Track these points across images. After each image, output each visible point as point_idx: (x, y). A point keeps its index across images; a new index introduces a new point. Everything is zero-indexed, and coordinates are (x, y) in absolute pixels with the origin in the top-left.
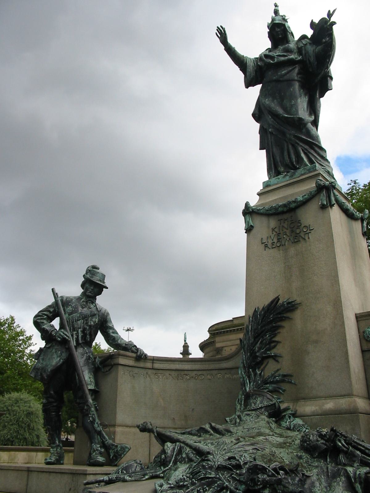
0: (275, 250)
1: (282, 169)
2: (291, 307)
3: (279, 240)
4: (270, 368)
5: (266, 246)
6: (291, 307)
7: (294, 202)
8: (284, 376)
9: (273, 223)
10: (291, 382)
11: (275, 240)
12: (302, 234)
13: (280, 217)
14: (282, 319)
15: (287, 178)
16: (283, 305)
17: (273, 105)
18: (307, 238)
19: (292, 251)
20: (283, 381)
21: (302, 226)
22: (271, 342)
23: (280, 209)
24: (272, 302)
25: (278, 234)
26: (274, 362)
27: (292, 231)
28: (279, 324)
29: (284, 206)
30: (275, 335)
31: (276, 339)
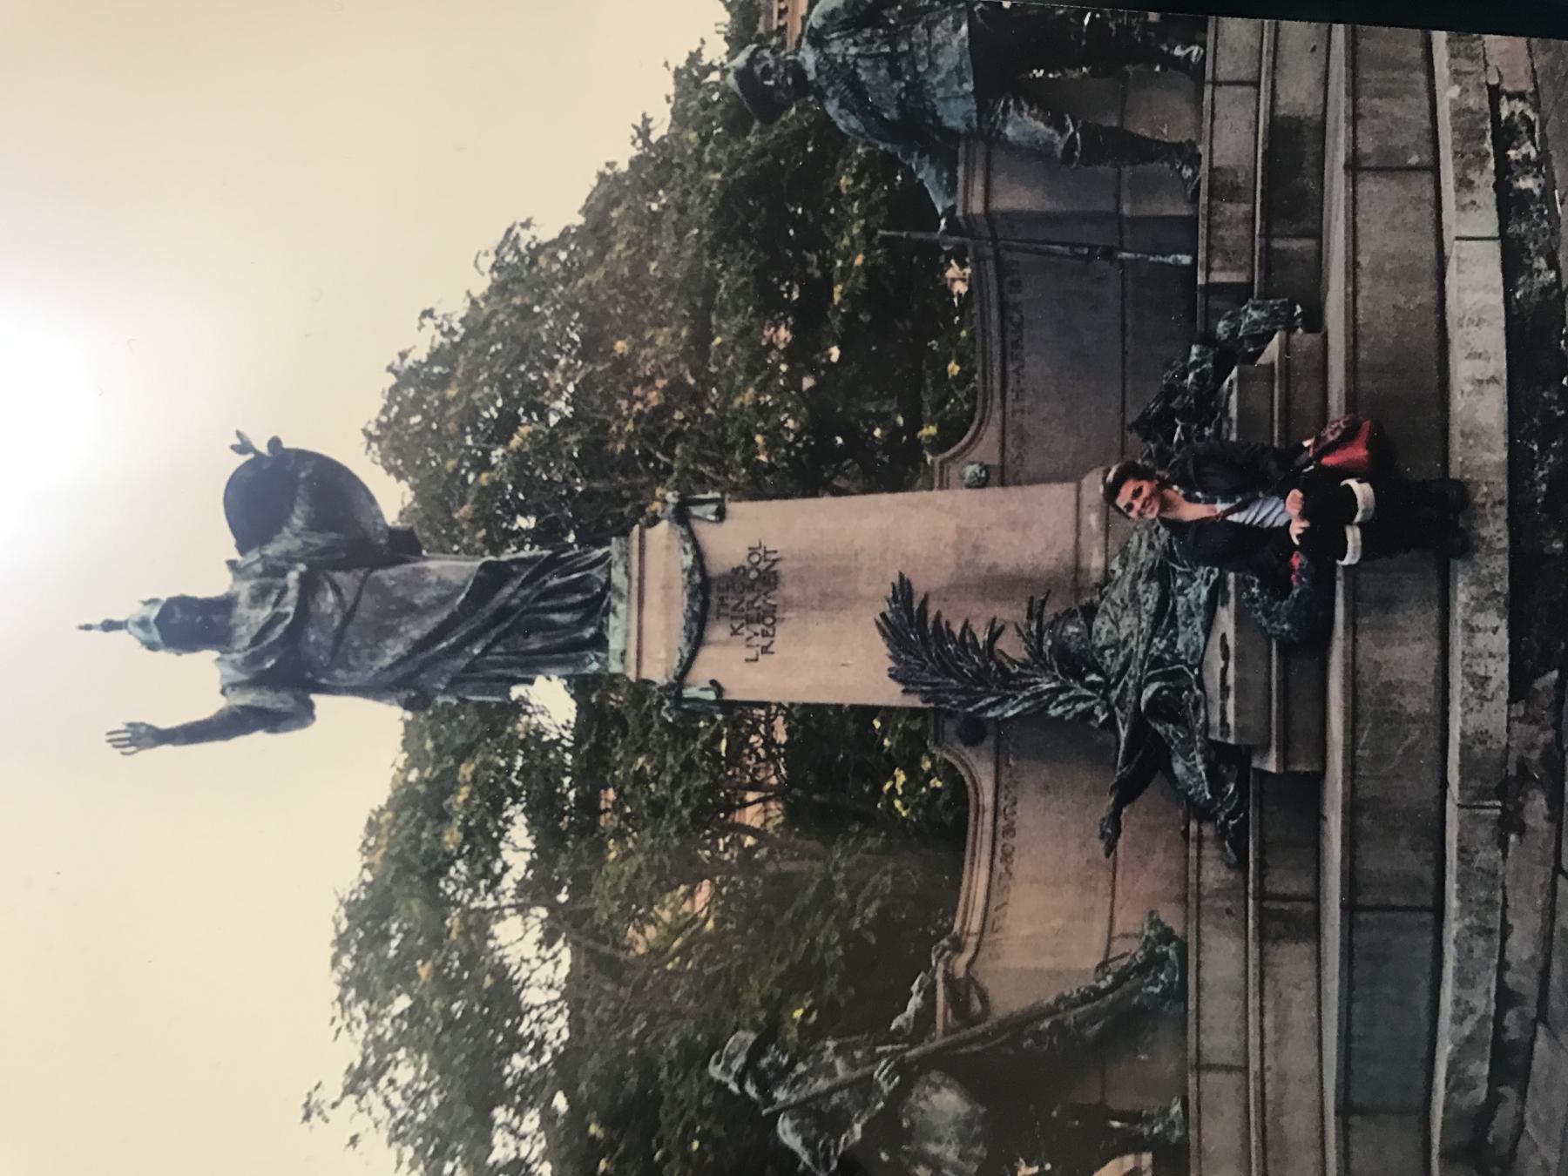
0: (779, 628)
1: (588, 632)
2: (903, 591)
3: (760, 620)
4: (1012, 647)
5: (765, 650)
6: (903, 591)
9: (718, 632)
11: (759, 628)
13: (712, 616)
15: (621, 607)
17: (416, 634)
19: (789, 590)
25: (749, 621)
26: (1003, 637)
29: (692, 596)
30: (951, 633)
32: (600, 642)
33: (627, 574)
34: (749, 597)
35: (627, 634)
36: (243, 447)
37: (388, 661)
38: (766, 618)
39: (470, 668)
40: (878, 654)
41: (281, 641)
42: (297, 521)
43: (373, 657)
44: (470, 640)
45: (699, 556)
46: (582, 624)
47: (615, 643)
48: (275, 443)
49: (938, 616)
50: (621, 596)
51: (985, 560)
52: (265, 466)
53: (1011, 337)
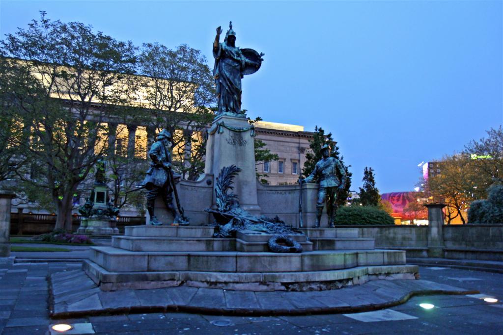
0: (232, 146)
1: (229, 108)
2: (239, 170)
3: (234, 142)
4: (229, 192)
5: (228, 143)
6: (239, 170)
8: (235, 195)
9: (232, 134)
11: (232, 142)
13: (235, 133)
14: (235, 174)
15: (234, 115)
17: (231, 78)
19: (239, 148)
20: (234, 197)
22: (230, 182)
23: (236, 130)
24: (232, 166)
25: (234, 140)
26: (231, 190)
29: (239, 129)
30: (231, 179)
31: (232, 181)
32: (227, 111)
33: (240, 117)
34: (238, 140)
35: (230, 116)
36: (262, 54)
37: (226, 73)
38: (234, 143)
39: (223, 86)
40: (228, 165)
41: (230, 56)
42: (247, 60)
43: (227, 71)
44: (229, 87)
45: (245, 131)
46: (231, 108)
47: (228, 113)
48: (263, 60)
49: (234, 177)
50: (236, 115)
51: (244, 186)
52: (259, 58)
53: (279, 192)
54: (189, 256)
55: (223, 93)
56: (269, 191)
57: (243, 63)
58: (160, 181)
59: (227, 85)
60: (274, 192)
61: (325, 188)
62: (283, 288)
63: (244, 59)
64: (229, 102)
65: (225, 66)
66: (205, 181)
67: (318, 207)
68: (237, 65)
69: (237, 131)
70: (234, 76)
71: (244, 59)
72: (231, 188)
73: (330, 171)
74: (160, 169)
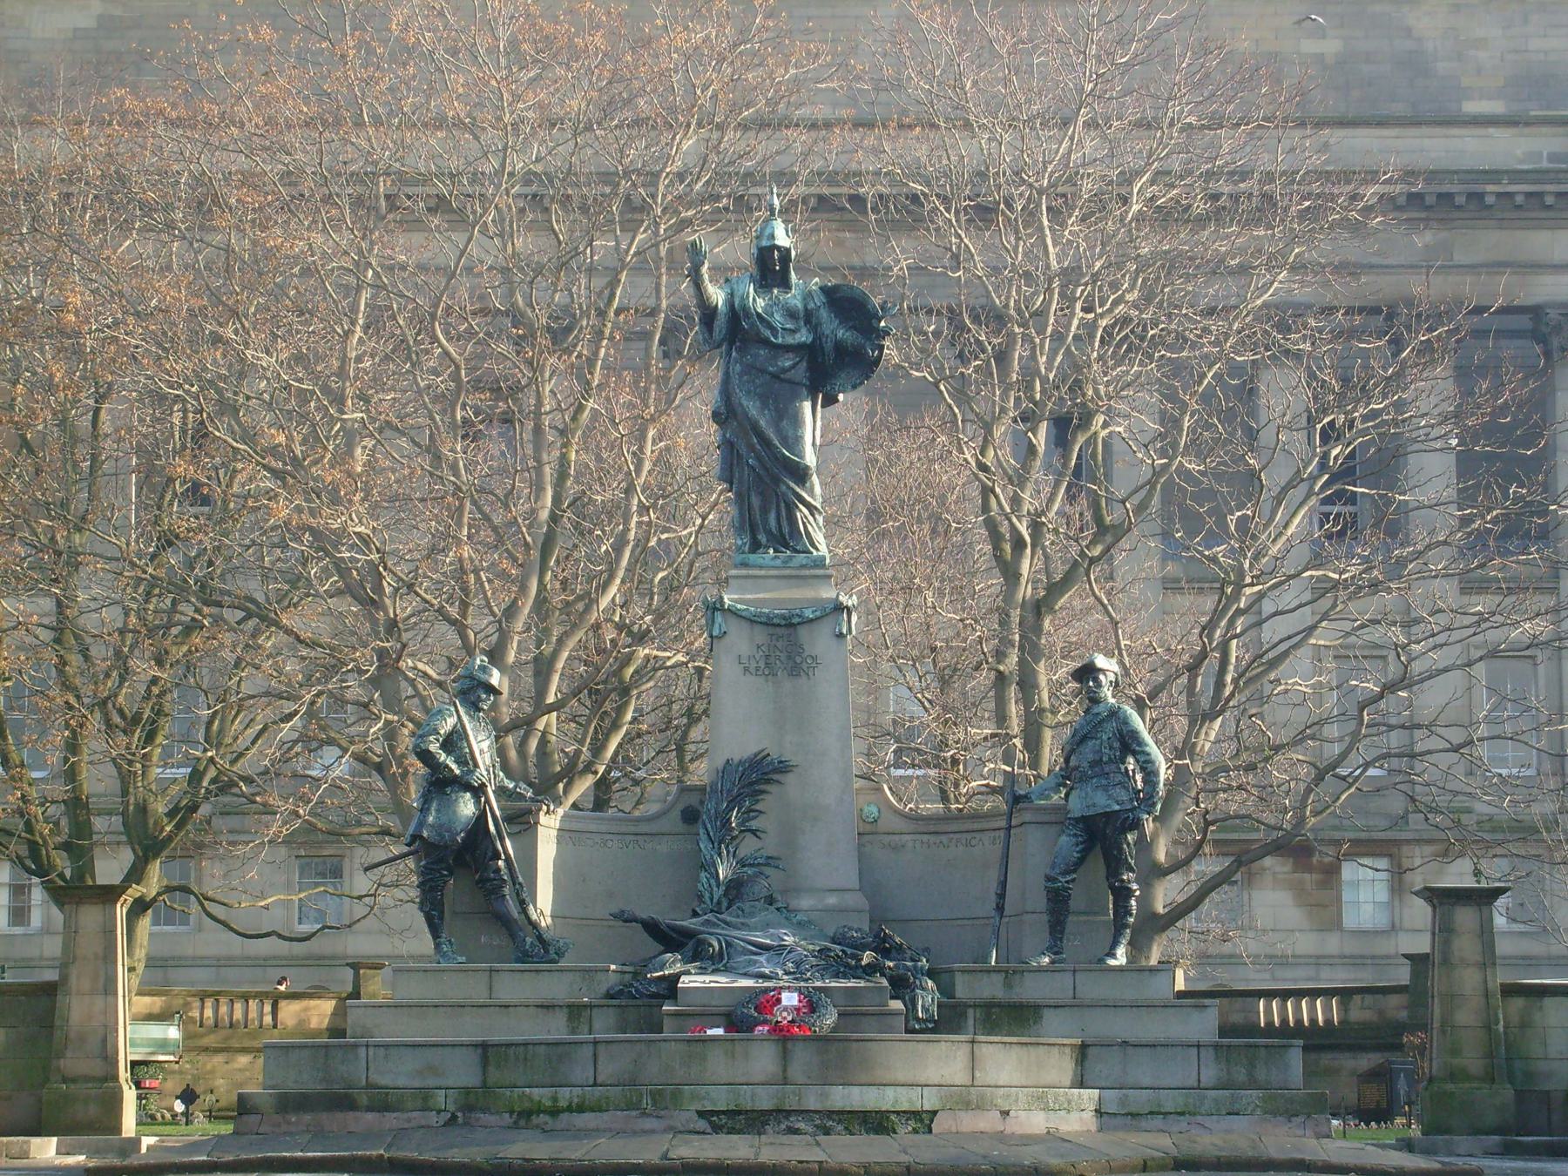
0: (761, 680)
1: (762, 538)
5: (746, 670)
6: (783, 768)
7: (800, 616)
9: (761, 635)
10: (777, 867)
12: (805, 666)
13: (771, 630)
14: (768, 781)
16: (772, 763)
17: (762, 423)
18: (811, 674)
20: (768, 865)
21: (805, 655)
23: (775, 621)
25: (767, 657)
27: (789, 658)
28: (763, 787)
29: (783, 617)
30: (758, 801)
31: (757, 807)
33: (803, 567)
34: (783, 656)
37: (745, 403)
38: (767, 668)
39: (739, 456)
41: (758, 333)
43: (749, 392)
44: (758, 458)
46: (769, 533)
54: (484, 1046)
55: (740, 482)
56: (925, 838)
57: (829, 346)
58: (449, 830)
59: (752, 448)
60: (944, 838)
61: (1077, 820)
62: (702, 1124)
63: (836, 331)
64: (765, 511)
65: (741, 375)
66: (676, 814)
67: (1049, 891)
68: (788, 364)
69: (779, 625)
70: (777, 409)
71: (836, 331)
72: (754, 832)
73: (1091, 757)
74: (448, 790)
